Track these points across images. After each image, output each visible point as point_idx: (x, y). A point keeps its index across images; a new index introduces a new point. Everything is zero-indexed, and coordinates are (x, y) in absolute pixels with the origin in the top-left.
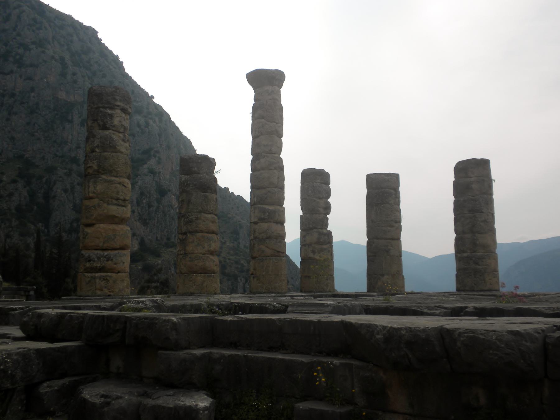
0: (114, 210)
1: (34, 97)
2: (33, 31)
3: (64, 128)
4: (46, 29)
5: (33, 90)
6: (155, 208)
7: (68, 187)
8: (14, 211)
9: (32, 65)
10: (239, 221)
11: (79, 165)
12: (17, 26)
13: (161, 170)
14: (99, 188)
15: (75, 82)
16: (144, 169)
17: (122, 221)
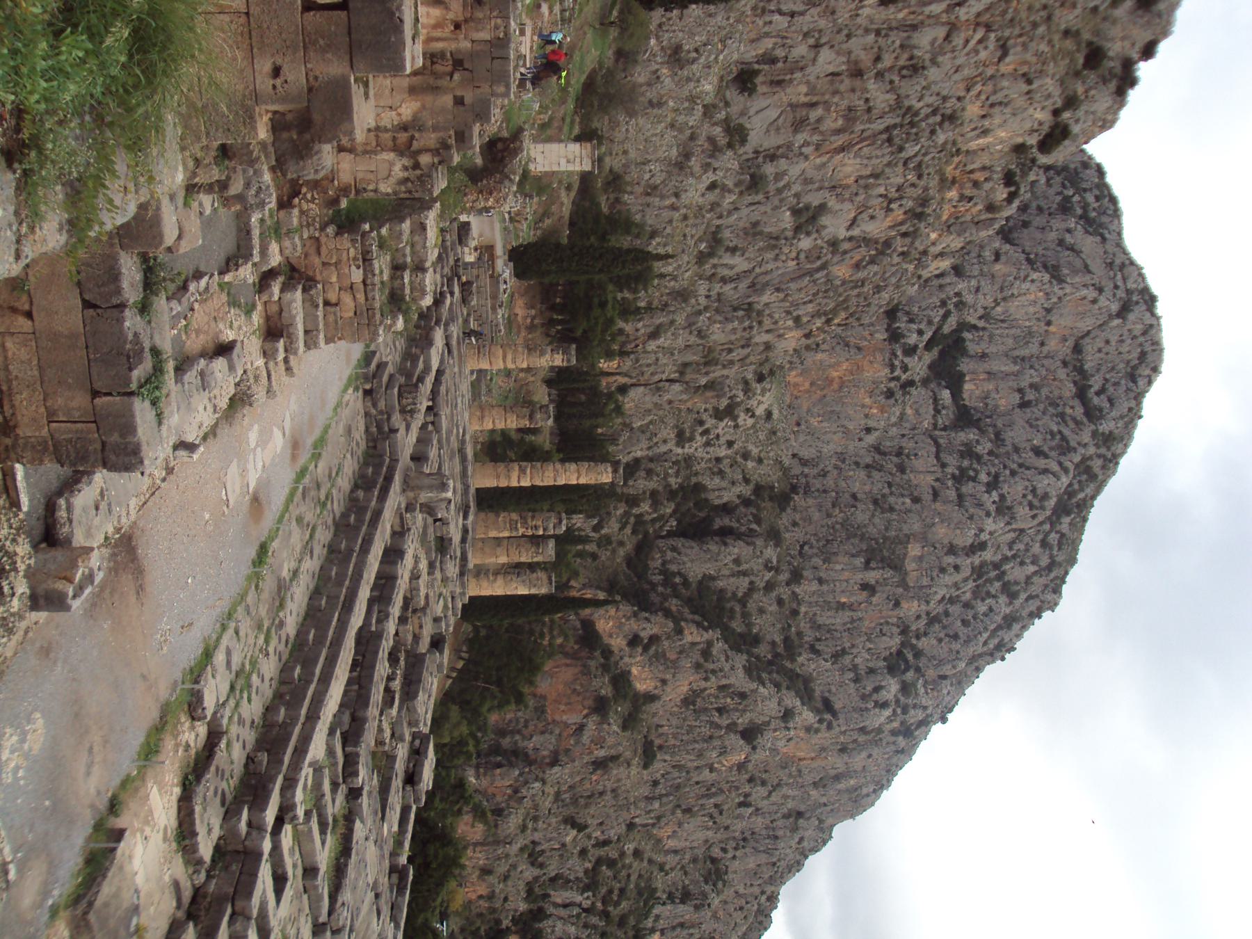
0: (509, 357)
1: (904, 503)
2: (1024, 496)
3: (853, 556)
4: (1034, 517)
5: (916, 500)
6: (716, 719)
7: (744, 567)
8: (694, 480)
9: (960, 497)
10: (709, 905)
11: (788, 584)
12: (1028, 468)
13: (792, 733)
14: (520, 349)
15: (943, 570)
16: (792, 701)
17: (504, 362)
